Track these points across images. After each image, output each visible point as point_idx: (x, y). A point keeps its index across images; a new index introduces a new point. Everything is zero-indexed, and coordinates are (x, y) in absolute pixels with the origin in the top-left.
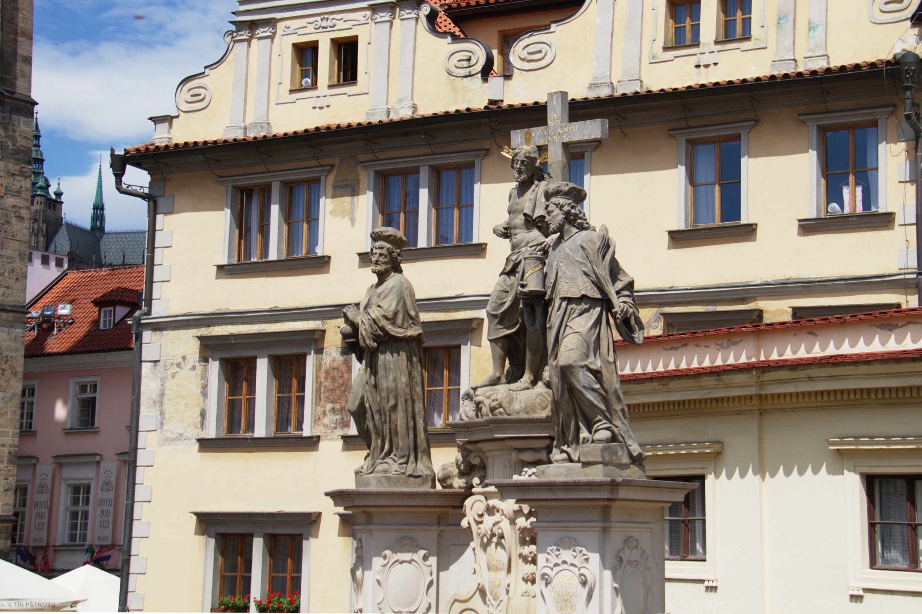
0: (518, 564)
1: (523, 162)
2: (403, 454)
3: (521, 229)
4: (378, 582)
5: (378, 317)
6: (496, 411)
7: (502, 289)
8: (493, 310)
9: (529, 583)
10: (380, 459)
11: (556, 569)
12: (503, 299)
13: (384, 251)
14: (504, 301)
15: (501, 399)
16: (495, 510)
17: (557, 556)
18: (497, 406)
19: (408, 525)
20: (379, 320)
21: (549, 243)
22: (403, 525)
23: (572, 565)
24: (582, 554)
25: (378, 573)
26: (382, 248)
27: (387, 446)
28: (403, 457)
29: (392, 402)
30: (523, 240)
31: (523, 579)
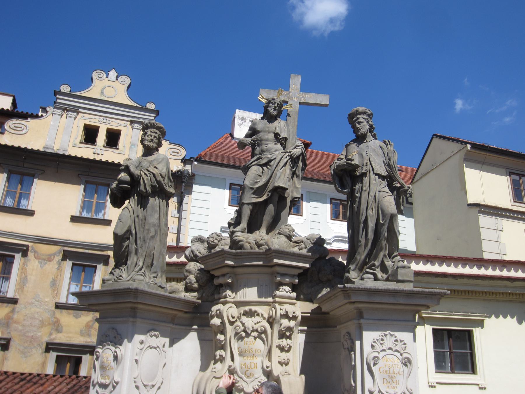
0: (276, 352)
1: (278, 104)
2: (155, 270)
3: (271, 141)
4: (136, 361)
5: (157, 173)
6: (263, 247)
7: (257, 173)
8: (251, 185)
9: (284, 365)
10: (135, 272)
11: (383, 353)
12: (257, 180)
13: (157, 135)
14: (258, 181)
15: (267, 239)
16: (256, 314)
17: (381, 344)
18: (264, 244)
19: (158, 321)
20: (158, 176)
21: (295, 153)
22: (155, 320)
23: (397, 351)
24: (403, 343)
25: (137, 354)
26: (156, 133)
27: (141, 264)
28: (155, 272)
29: (152, 233)
30: (273, 148)
31: (280, 363)
